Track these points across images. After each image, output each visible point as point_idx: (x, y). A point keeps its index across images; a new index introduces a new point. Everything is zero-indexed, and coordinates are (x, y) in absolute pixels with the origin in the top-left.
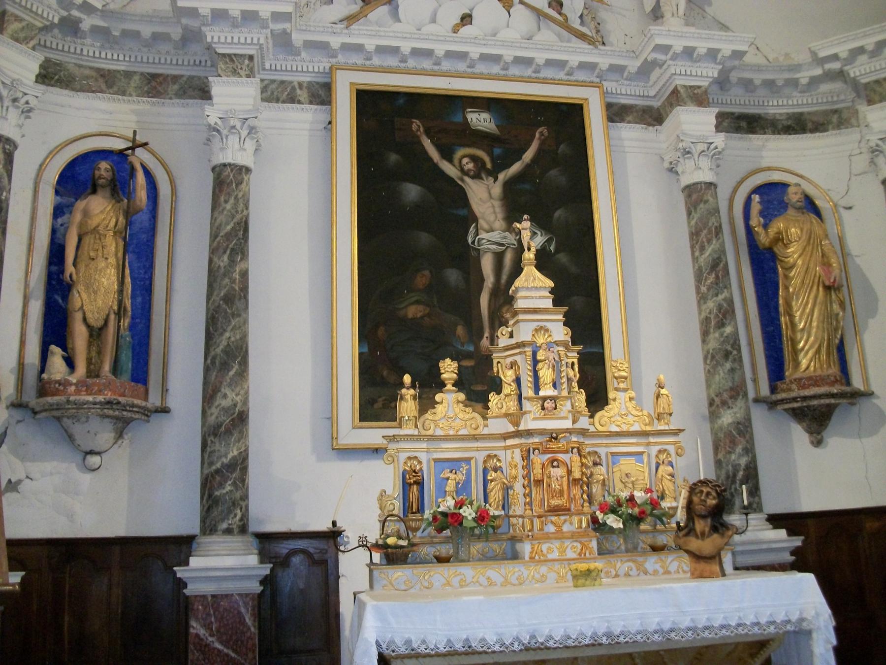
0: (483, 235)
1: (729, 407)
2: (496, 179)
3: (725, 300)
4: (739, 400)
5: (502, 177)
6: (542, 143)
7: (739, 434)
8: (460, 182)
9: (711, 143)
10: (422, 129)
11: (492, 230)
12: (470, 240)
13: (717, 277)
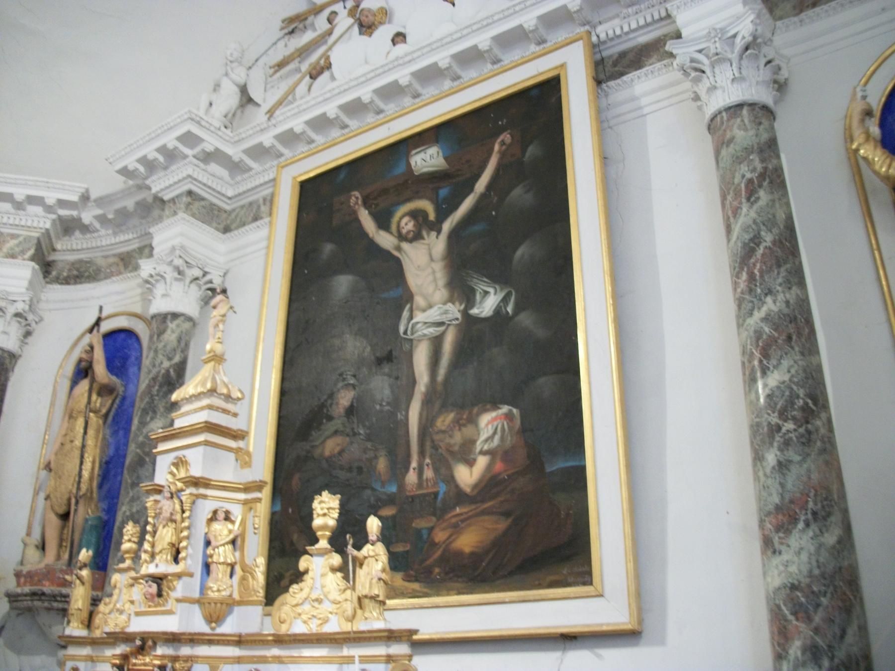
0: (419, 317)
1: (774, 552)
2: (439, 231)
3: (765, 319)
4: (795, 534)
5: (447, 226)
6: (503, 154)
7: (795, 613)
8: (396, 253)
9: (735, 36)
10: (360, 202)
11: (430, 306)
12: (402, 329)
13: (751, 277)
